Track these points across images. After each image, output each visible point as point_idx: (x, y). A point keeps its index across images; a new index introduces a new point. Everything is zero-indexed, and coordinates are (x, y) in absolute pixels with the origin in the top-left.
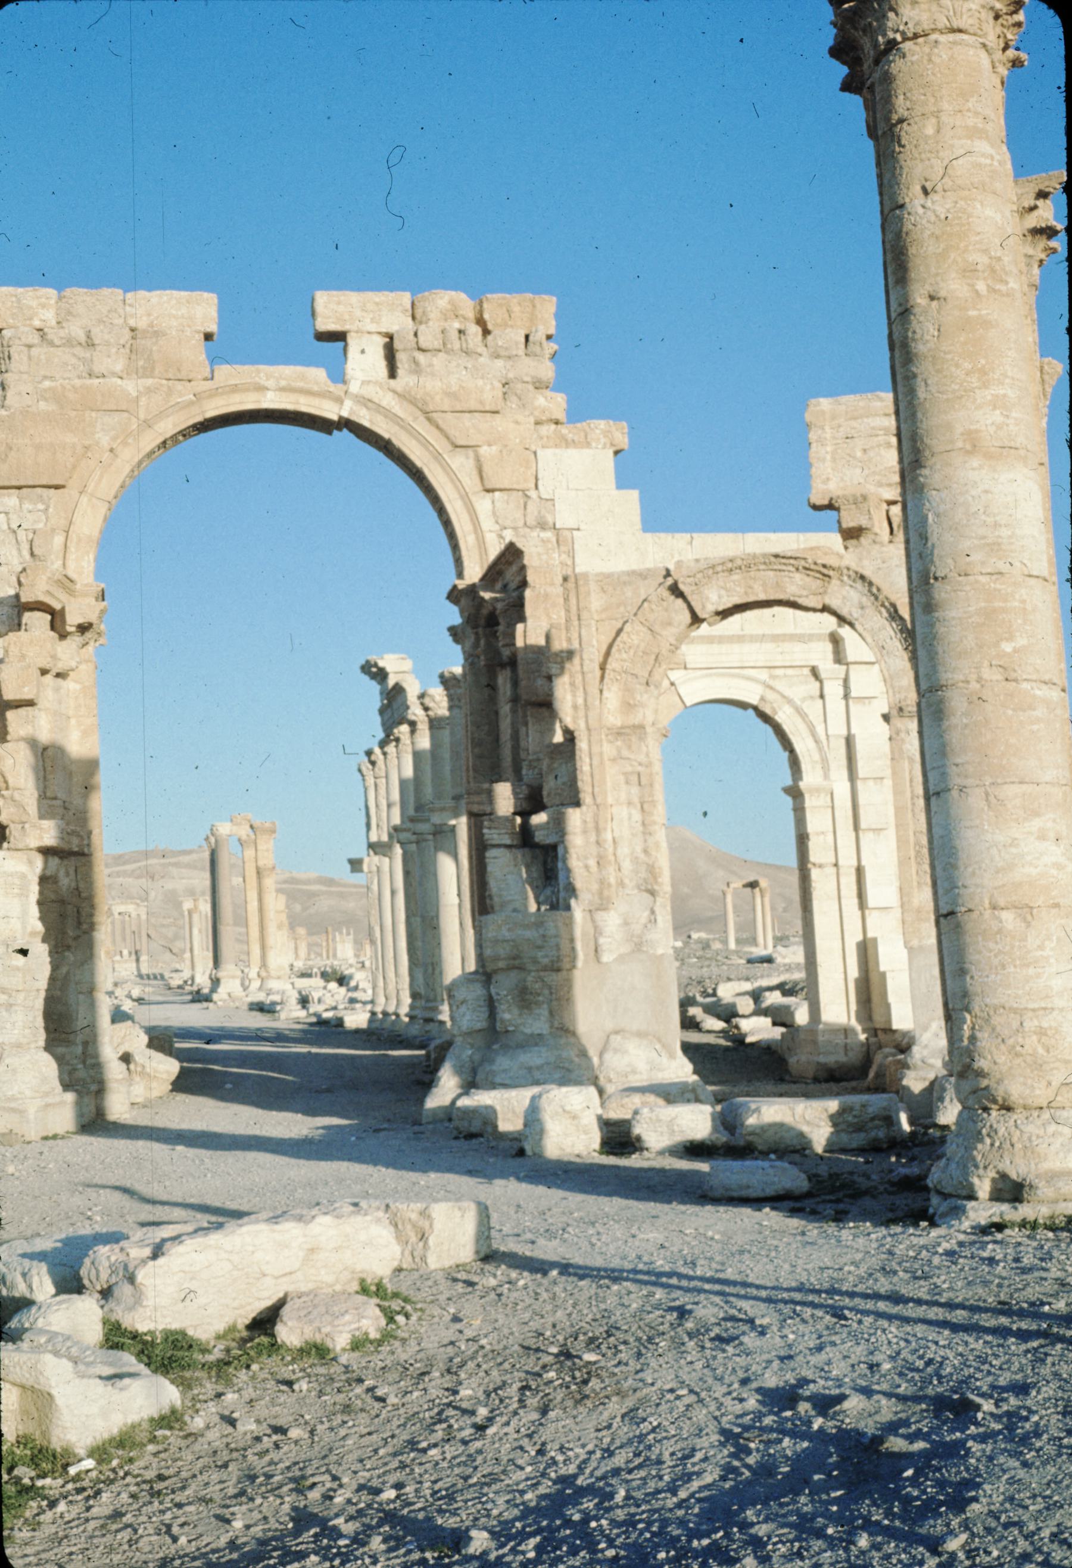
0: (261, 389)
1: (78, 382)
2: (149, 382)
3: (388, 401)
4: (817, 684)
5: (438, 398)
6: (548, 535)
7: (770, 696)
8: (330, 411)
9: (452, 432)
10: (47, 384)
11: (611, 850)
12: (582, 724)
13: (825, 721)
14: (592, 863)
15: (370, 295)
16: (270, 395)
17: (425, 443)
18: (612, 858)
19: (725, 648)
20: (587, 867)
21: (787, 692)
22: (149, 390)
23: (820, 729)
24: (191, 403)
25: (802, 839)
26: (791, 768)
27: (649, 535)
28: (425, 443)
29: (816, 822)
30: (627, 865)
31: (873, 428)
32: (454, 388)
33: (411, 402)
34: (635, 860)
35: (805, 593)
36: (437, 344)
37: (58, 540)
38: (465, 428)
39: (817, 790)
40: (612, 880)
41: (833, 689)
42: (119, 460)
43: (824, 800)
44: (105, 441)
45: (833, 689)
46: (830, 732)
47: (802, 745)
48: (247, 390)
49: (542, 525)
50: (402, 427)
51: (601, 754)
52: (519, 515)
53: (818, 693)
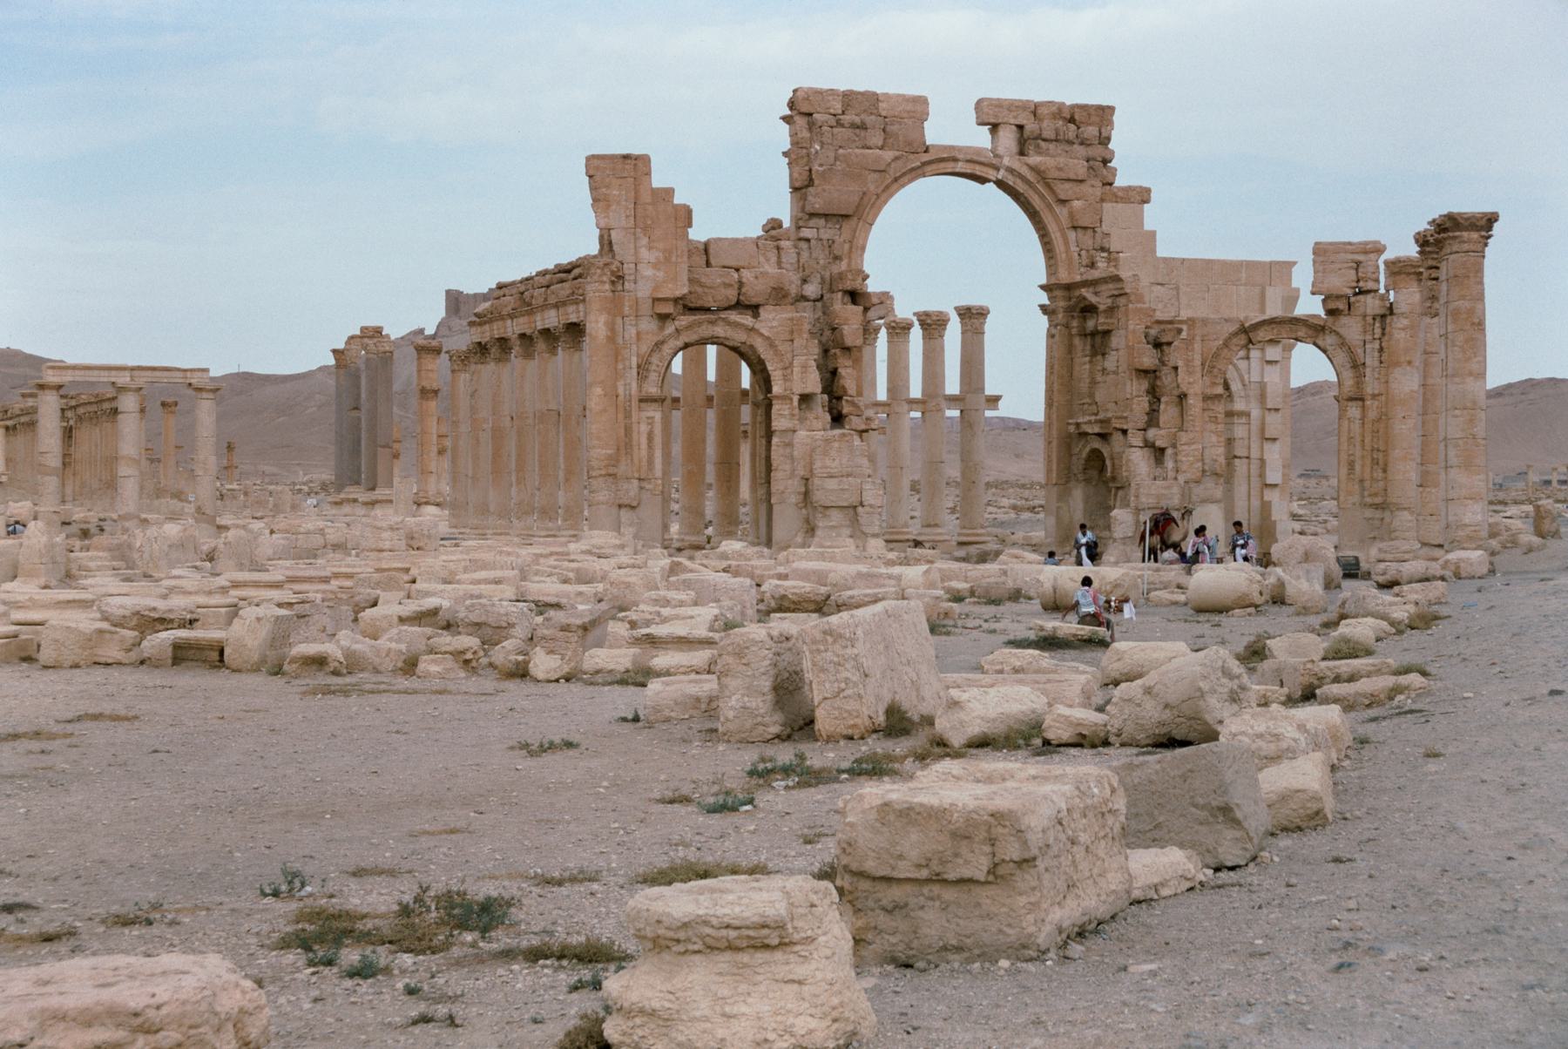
0: (955, 160)
3: (1025, 171)
6: (1105, 255)
8: (991, 174)
9: (1058, 191)
10: (841, 151)
16: (960, 164)
17: (1042, 197)
22: (897, 158)
23: (1246, 377)
24: (919, 167)
37: (847, 246)
38: (1064, 190)
39: (1241, 414)
49: (1103, 249)
52: (1090, 242)
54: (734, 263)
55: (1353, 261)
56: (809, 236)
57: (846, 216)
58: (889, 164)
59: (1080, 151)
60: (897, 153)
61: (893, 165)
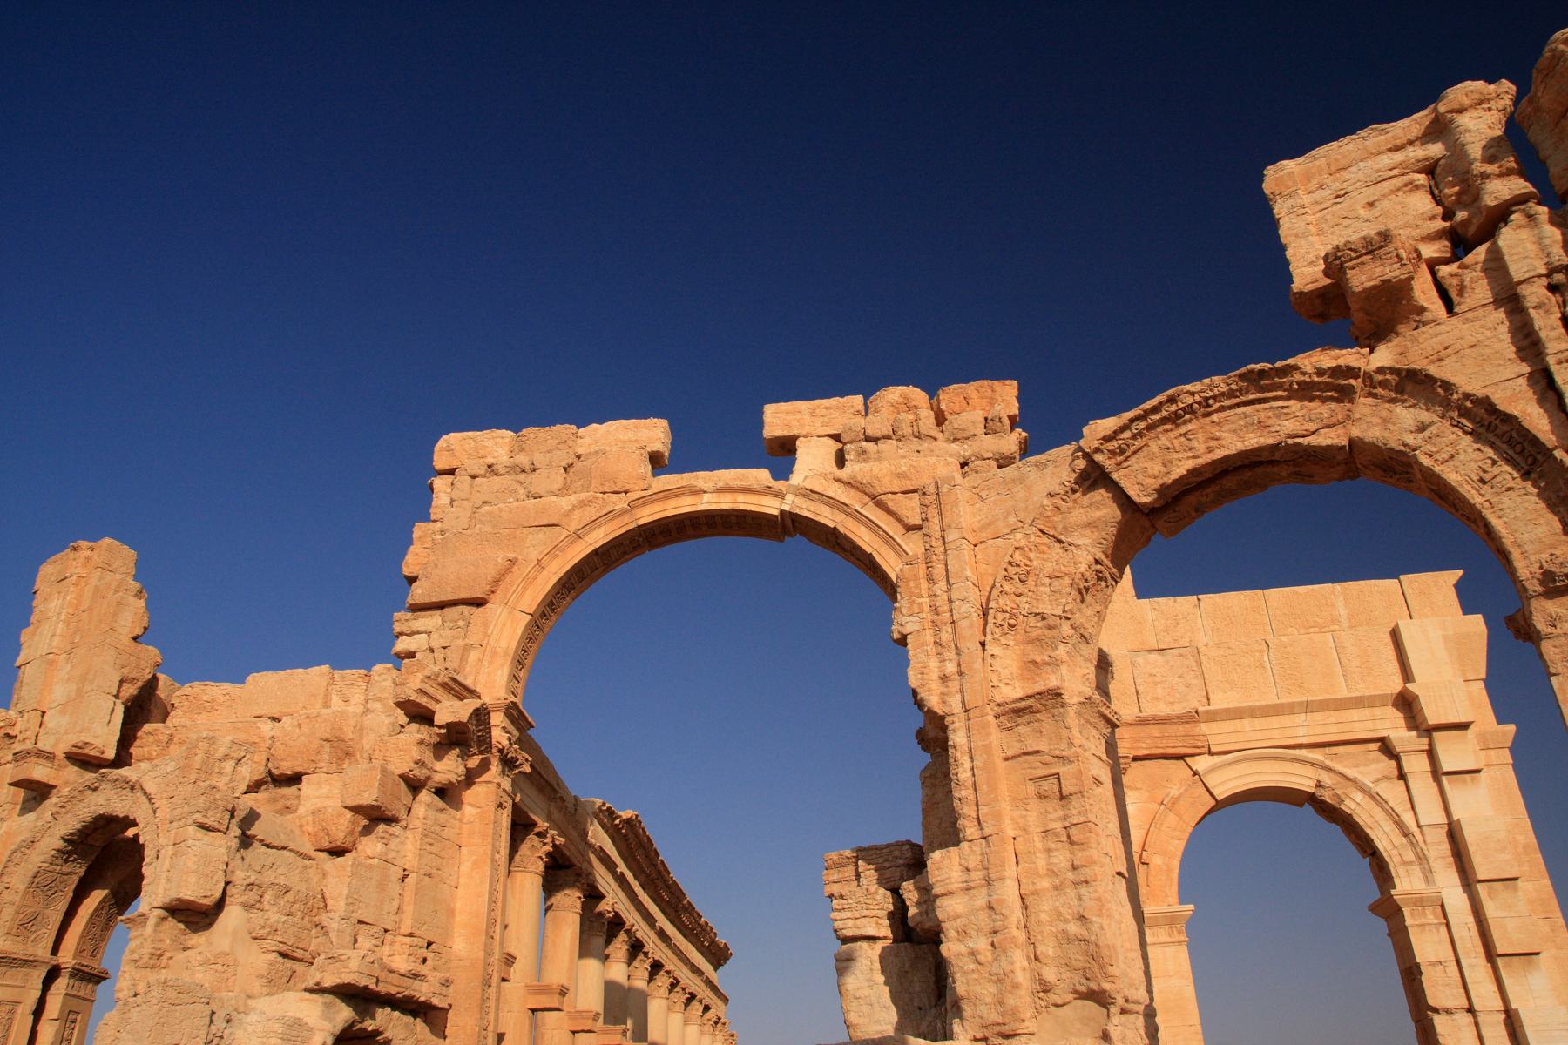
0: (699, 492)
1: (516, 504)
2: (583, 496)
4: (1393, 763)
5: (886, 480)
7: (1326, 778)
8: (770, 506)
10: (486, 508)
11: (1016, 915)
12: (955, 704)
13: (1413, 808)
14: (982, 944)
15: (818, 402)
17: (873, 526)
18: (1021, 936)
19: (1258, 723)
20: (973, 953)
21: (1350, 773)
22: (583, 504)
23: (1408, 818)
24: (624, 512)
25: (1411, 974)
26: (1377, 878)
27: (1145, 602)
28: (873, 526)
29: (1427, 947)
30: (1048, 949)
31: (1378, 171)
32: (904, 468)
33: (857, 488)
34: (1065, 938)
35: (1312, 427)
36: (887, 430)
39: (1419, 901)
40: (1022, 977)
41: (1416, 765)
42: (545, 572)
43: (1432, 917)
44: (534, 555)
45: (1416, 765)
46: (1422, 822)
47: (1384, 838)
48: (683, 495)
50: (848, 514)
51: (987, 749)
53: (1396, 773)
54: (276, 713)
55: (1404, 168)
56: (412, 647)
57: (479, 603)
58: (569, 513)
59: (942, 445)
60: (583, 496)
61: (577, 514)
